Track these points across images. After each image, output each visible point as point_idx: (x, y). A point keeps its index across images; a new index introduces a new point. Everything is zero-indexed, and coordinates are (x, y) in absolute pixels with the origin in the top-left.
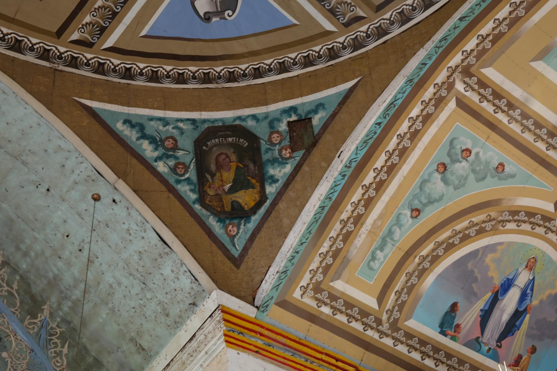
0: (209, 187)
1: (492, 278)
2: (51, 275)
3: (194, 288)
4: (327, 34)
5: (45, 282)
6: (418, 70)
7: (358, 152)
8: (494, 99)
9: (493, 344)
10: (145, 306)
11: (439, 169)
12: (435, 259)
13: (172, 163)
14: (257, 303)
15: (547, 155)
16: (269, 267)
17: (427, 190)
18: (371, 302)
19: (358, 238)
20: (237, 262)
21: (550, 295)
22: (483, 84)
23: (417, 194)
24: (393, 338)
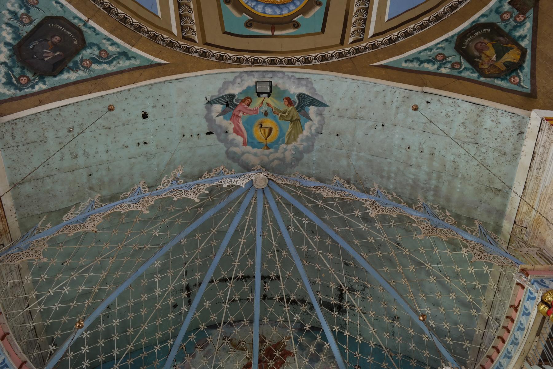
0: (482, 65)
2: (410, 181)
3: (515, 120)
5: (409, 188)
10: (485, 159)
13: (449, 65)
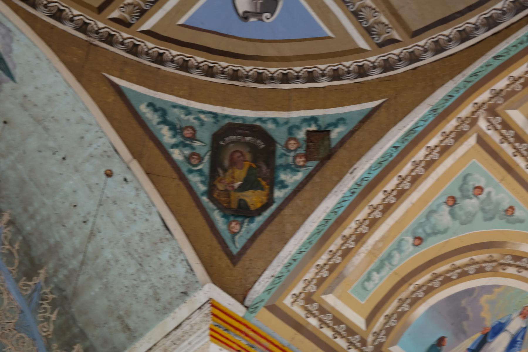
1: (484, 319)
4: (359, 51)
7: (372, 172)
10: (137, 287)
12: (430, 290)
13: (187, 152)
14: (248, 302)
16: (265, 269)
18: (359, 321)
20: (234, 259)
22: (506, 125)
23: (421, 223)
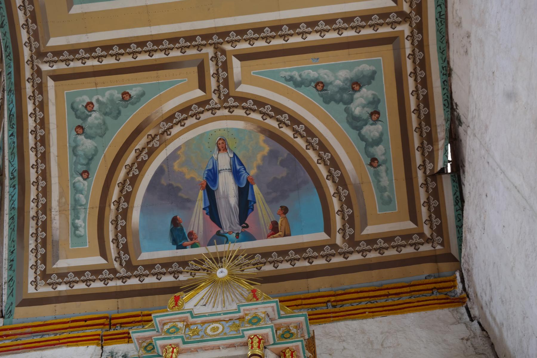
1: (192, 179)
6: (9, 81)
8: (74, 56)
9: (238, 228)
11: (79, 132)
12: (128, 197)
15: (156, 60)
17: (80, 153)
18: (97, 260)
19: (54, 222)
21: (264, 158)
22: (58, 53)
24: (136, 276)
